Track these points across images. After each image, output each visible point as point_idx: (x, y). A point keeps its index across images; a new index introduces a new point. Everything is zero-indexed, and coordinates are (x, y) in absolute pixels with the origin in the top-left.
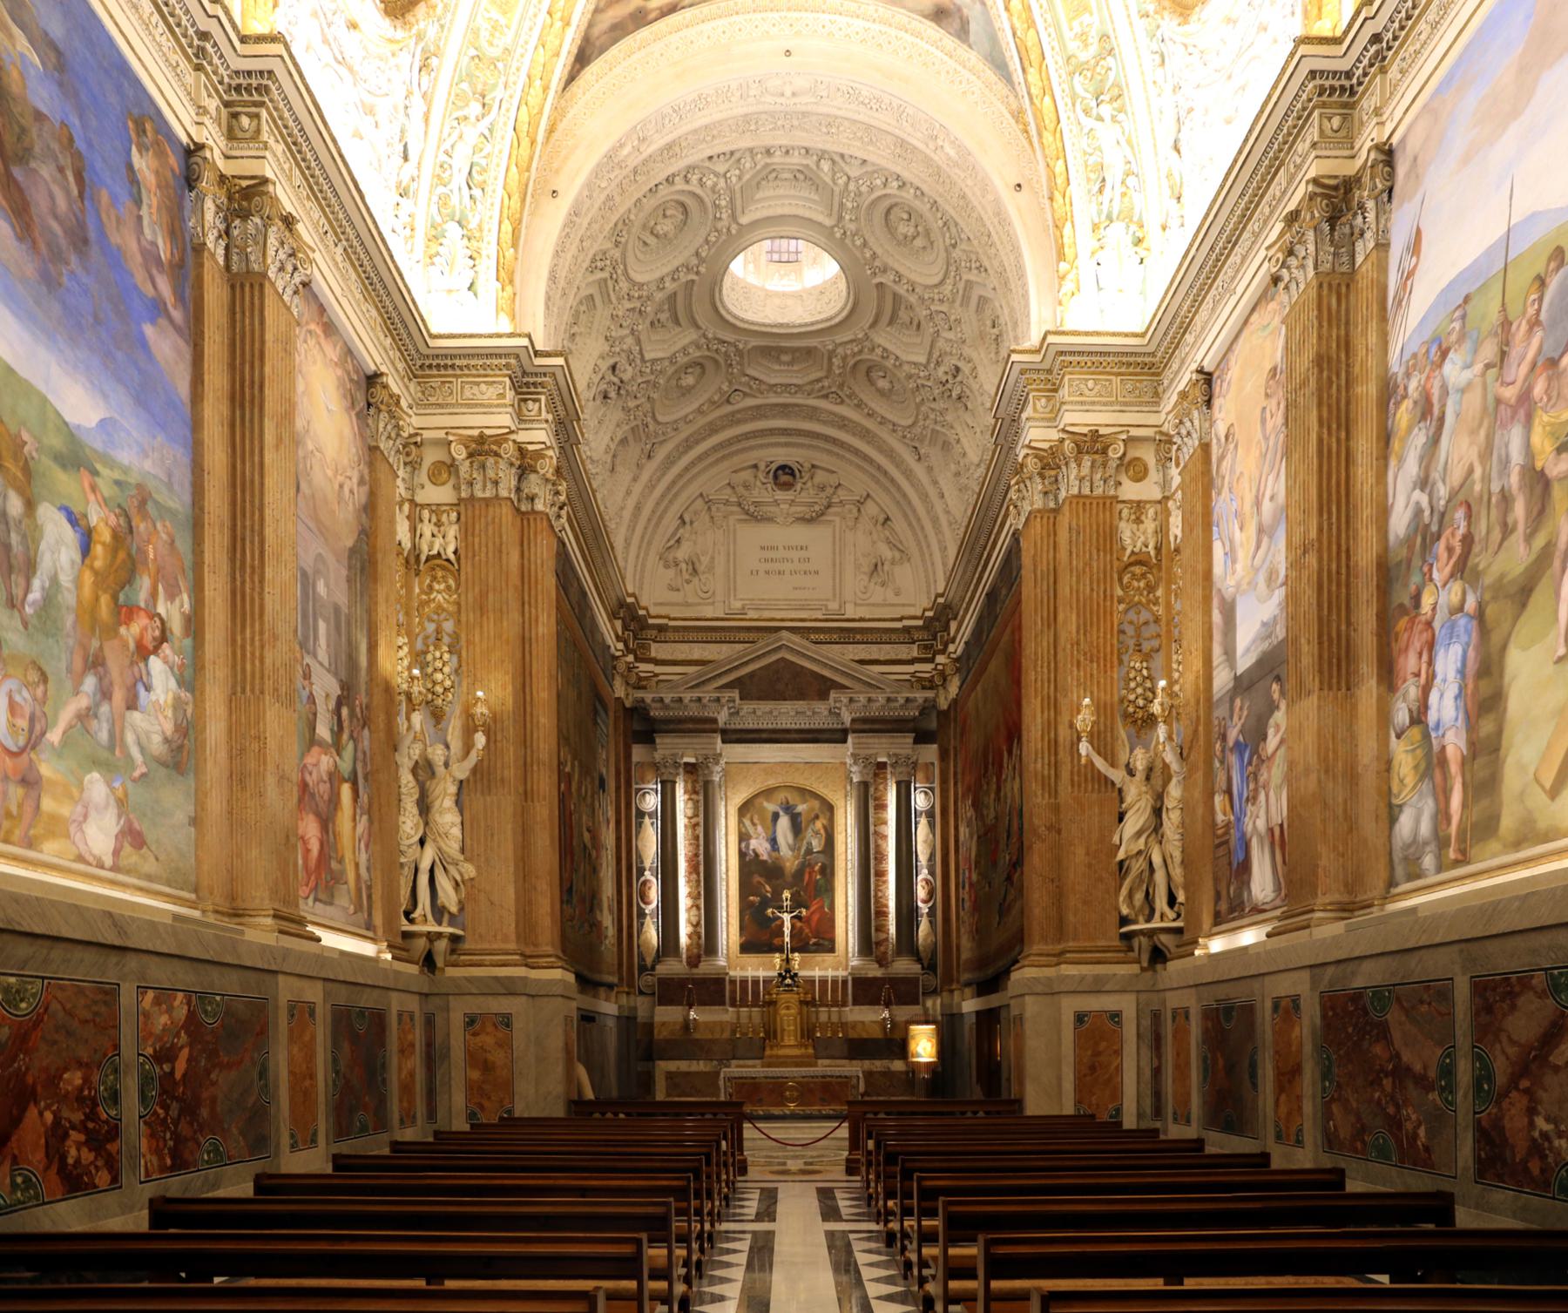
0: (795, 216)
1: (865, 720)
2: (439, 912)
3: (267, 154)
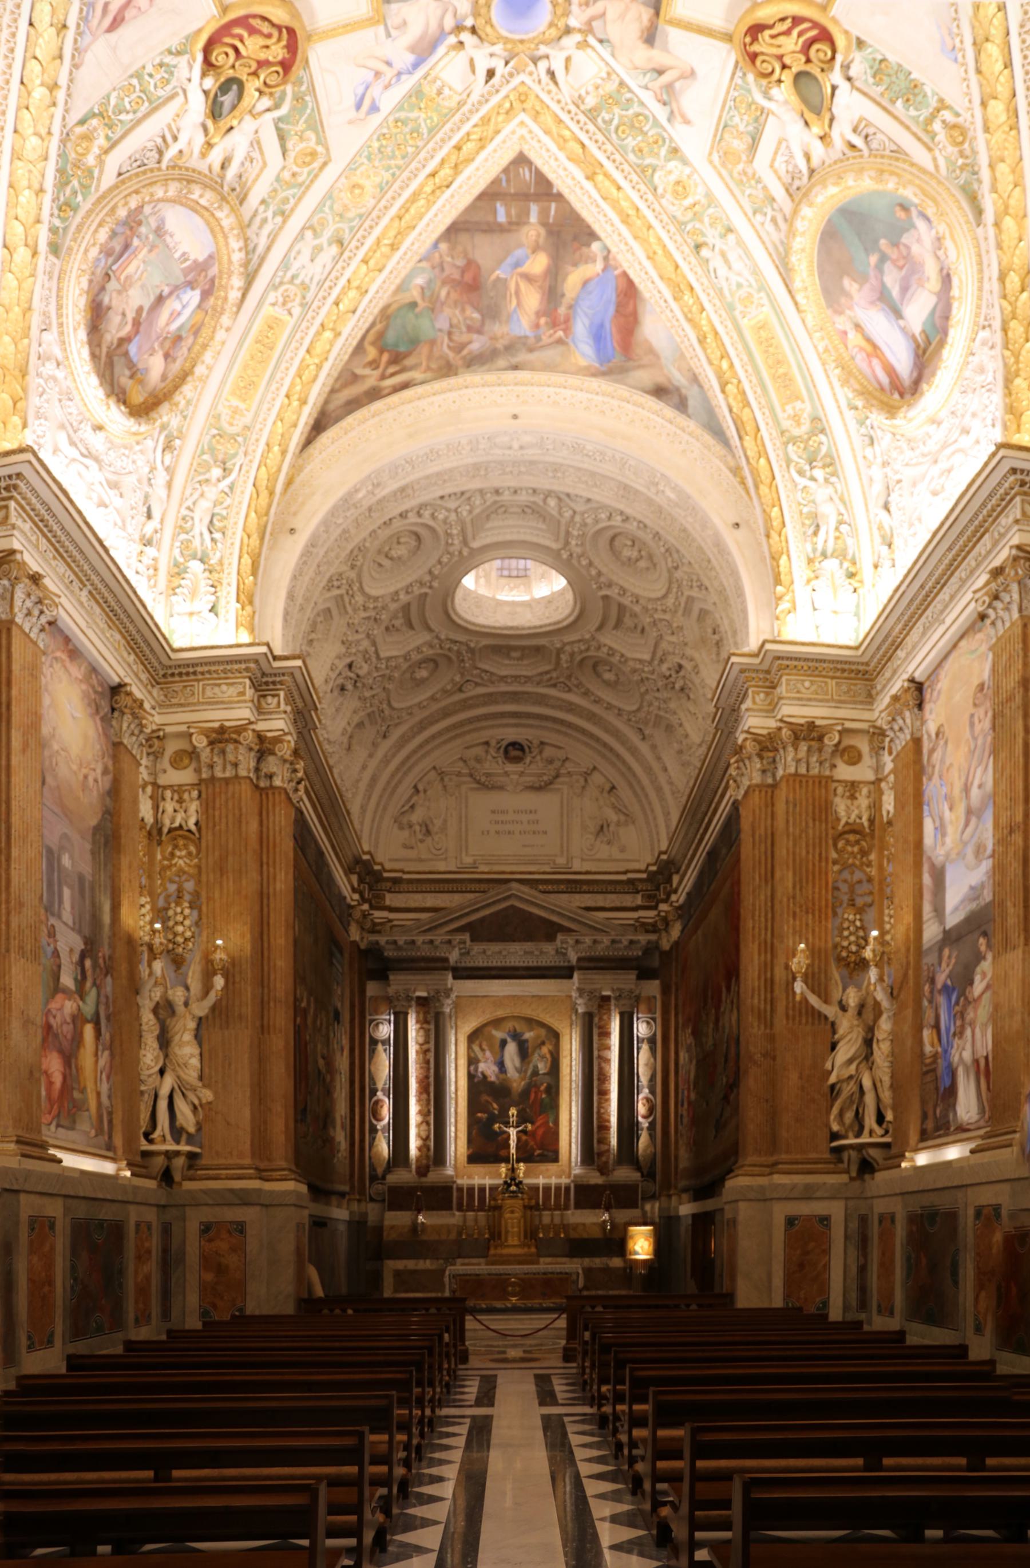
1: (590, 959)
2: (177, 1132)
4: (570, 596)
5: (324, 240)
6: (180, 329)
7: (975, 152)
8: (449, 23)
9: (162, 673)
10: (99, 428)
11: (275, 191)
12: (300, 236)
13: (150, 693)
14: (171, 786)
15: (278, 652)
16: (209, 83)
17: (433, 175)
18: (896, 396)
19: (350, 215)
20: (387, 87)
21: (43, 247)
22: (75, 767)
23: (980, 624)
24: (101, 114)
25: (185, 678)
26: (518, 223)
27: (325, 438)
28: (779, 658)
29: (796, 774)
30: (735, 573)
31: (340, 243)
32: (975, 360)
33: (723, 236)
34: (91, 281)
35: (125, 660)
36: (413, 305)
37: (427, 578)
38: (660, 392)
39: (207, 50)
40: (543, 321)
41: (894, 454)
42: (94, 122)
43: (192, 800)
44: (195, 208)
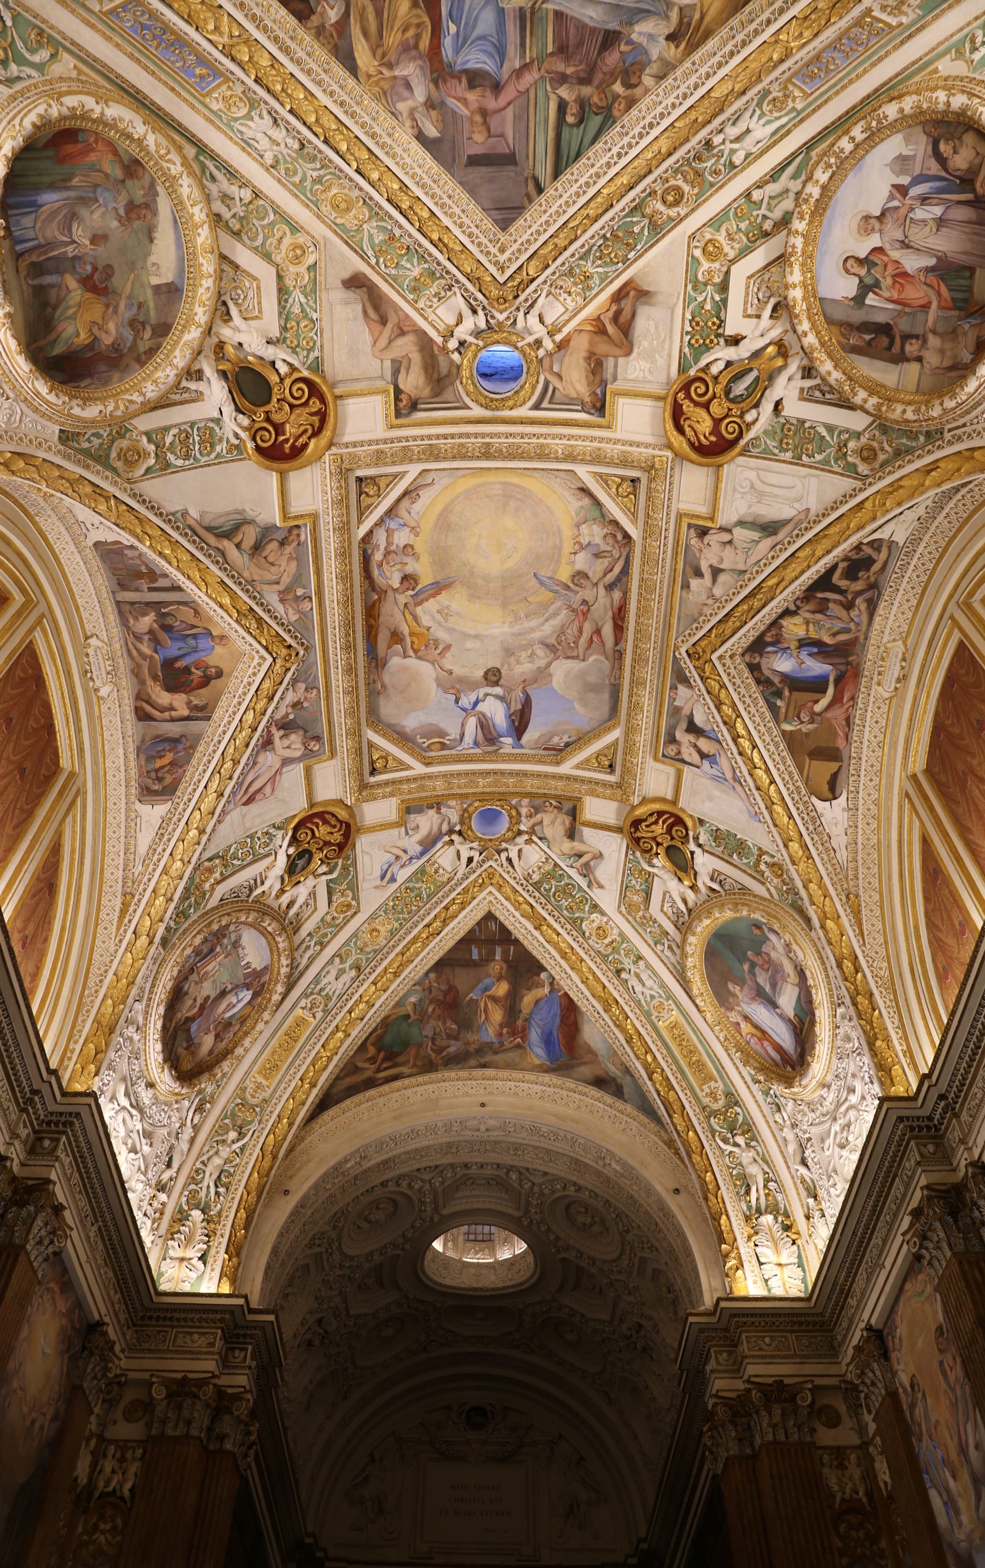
0: (489, 1210)
3: (57, 1164)
4: (531, 1259)
5: (347, 965)
6: (231, 1017)
7: (792, 880)
8: (445, 828)
9: (141, 1314)
10: (151, 1085)
11: (319, 928)
12: (331, 961)
13: (124, 1334)
14: (116, 1441)
15: (254, 1305)
16: (291, 851)
17: (428, 926)
18: (789, 1069)
19: (368, 949)
20: (402, 867)
21: (157, 939)
22: (25, 1410)
23: (917, 1265)
24: (223, 857)
25: (161, 1323)
26: (489, 958)
27: (326, 1116)
28: (735, 1315)
29: (775, 1442)
30: (681, 1235)
31: (358, 968)
32: (841, 1031)
33: (635, 963)
34: (180, 971)
35: (110, 1299)
36: (407, 1016)
37: (401, 1241)
38: (600, 1082)
39: (296, 829)
40: (505, 1031)
41: (799, 1117)
42: (217, 861)
43: (134, 1460)
44: (263, 932)
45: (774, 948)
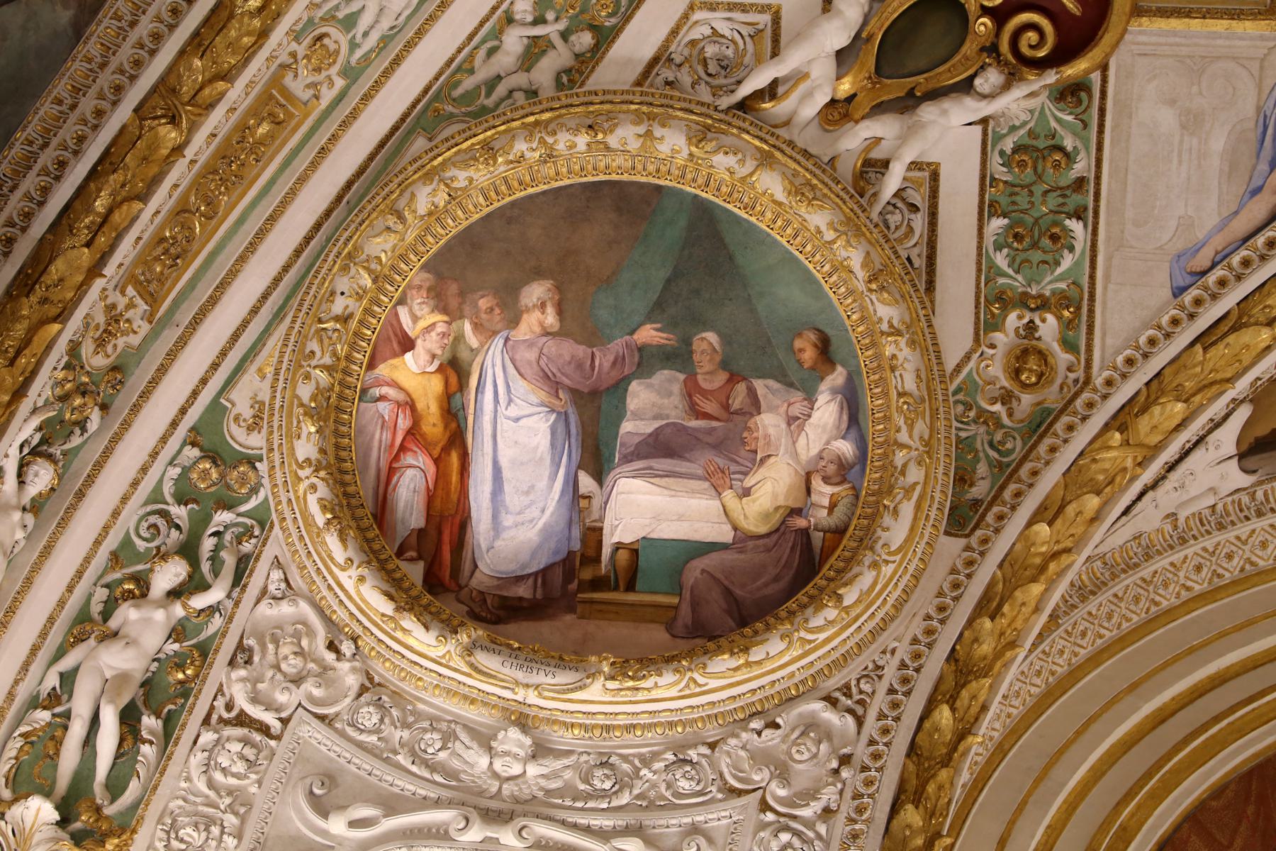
45: (795, 422)
